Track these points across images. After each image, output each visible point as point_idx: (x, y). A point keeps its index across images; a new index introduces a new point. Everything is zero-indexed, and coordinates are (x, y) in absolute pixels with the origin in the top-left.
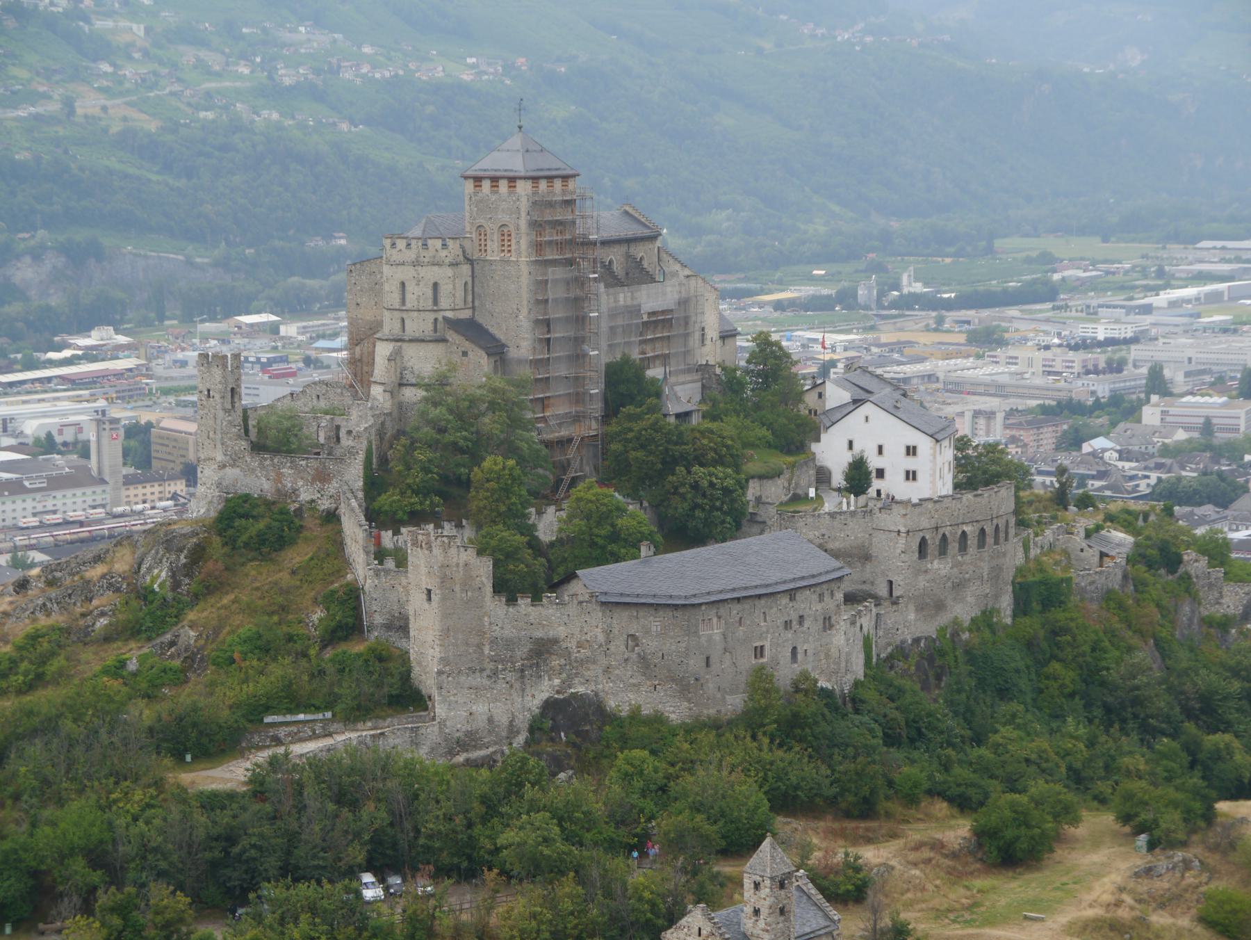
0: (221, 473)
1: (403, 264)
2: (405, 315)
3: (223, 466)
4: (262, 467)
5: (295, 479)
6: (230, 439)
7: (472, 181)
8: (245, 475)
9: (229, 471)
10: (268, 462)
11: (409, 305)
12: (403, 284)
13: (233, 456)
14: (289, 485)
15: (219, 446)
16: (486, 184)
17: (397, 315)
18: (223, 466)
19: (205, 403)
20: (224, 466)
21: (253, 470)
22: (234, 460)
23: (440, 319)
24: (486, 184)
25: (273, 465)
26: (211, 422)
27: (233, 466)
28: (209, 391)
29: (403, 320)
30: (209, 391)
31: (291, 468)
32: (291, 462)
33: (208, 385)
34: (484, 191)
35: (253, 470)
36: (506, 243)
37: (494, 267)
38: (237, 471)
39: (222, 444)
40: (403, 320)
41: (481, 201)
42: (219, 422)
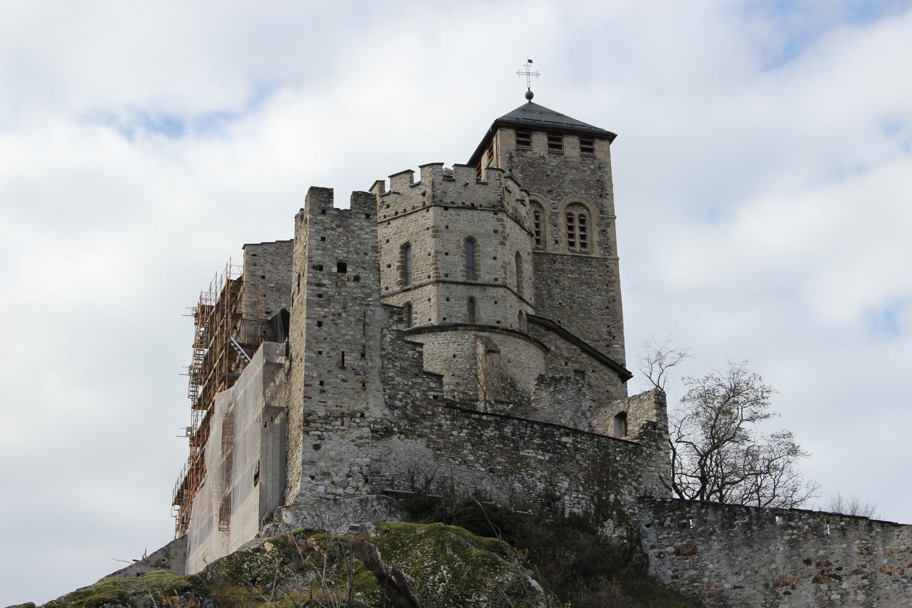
0: (381, 447)
1: (473, 207)
2: (476, 293)
3: (383, 432)
4: (478, 444)
5: (553, 474)
6: (403, 372)
7: (512, 132)
8: (437, 458)
9: (396, 442)
10: (489, 432)
11: (485, 276)
12: (471, 241)
13: (409, 411)
14: (541, 486)
15: (375, 384)
16: (540, 142)
17: (462, 292)
18: (383, 432)
19: (331, 291)
20: (387, 433)
21: (456, 447)
22: (413, 421)
23: (524, 313)
24: (540, 142)
25: (502, 438)
26: (352, 333)
27: (407, 434)
28: (342, 267)
29: (472, 301)
30: (342, 267)
31: (542, 448)
32: (543, 437)
33: (341, 254)
34: (536, 150)
35: (456, 447)
36: (577, 232)
37: (558, 266)
38: (418, 446)
39: (383, 382)
40: (472, 301)
41: (531, 165)
42: (374, 331)
